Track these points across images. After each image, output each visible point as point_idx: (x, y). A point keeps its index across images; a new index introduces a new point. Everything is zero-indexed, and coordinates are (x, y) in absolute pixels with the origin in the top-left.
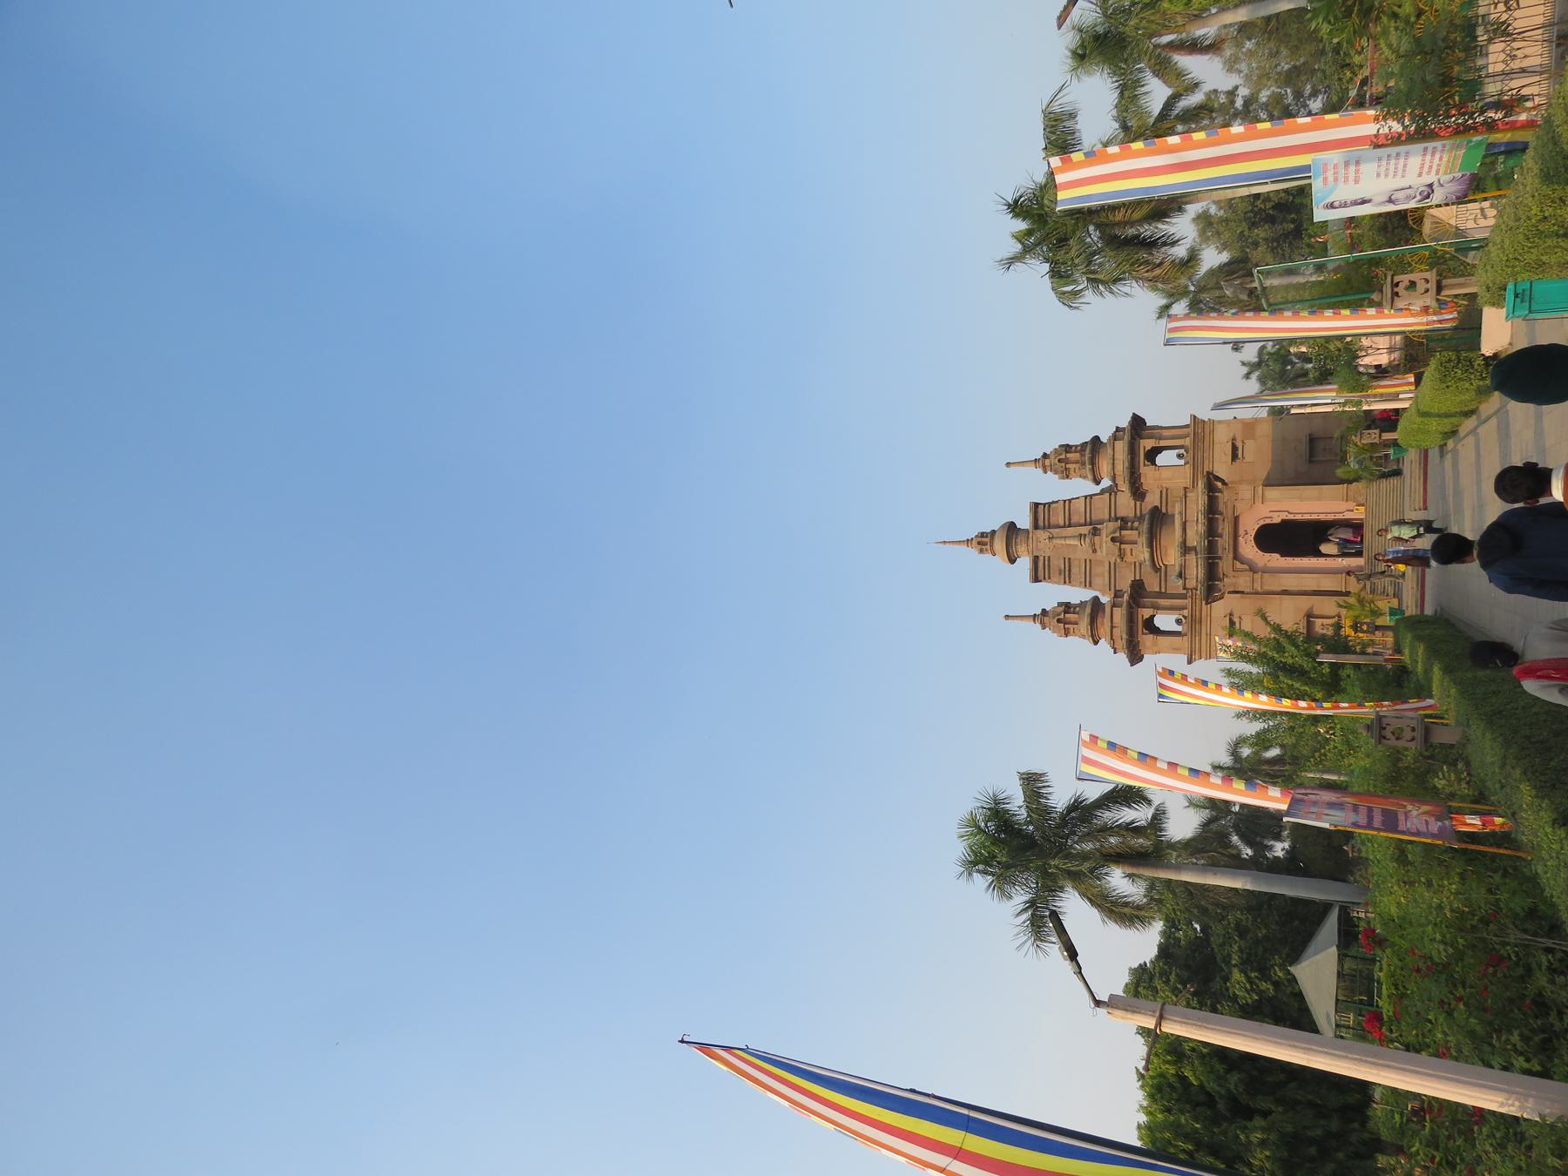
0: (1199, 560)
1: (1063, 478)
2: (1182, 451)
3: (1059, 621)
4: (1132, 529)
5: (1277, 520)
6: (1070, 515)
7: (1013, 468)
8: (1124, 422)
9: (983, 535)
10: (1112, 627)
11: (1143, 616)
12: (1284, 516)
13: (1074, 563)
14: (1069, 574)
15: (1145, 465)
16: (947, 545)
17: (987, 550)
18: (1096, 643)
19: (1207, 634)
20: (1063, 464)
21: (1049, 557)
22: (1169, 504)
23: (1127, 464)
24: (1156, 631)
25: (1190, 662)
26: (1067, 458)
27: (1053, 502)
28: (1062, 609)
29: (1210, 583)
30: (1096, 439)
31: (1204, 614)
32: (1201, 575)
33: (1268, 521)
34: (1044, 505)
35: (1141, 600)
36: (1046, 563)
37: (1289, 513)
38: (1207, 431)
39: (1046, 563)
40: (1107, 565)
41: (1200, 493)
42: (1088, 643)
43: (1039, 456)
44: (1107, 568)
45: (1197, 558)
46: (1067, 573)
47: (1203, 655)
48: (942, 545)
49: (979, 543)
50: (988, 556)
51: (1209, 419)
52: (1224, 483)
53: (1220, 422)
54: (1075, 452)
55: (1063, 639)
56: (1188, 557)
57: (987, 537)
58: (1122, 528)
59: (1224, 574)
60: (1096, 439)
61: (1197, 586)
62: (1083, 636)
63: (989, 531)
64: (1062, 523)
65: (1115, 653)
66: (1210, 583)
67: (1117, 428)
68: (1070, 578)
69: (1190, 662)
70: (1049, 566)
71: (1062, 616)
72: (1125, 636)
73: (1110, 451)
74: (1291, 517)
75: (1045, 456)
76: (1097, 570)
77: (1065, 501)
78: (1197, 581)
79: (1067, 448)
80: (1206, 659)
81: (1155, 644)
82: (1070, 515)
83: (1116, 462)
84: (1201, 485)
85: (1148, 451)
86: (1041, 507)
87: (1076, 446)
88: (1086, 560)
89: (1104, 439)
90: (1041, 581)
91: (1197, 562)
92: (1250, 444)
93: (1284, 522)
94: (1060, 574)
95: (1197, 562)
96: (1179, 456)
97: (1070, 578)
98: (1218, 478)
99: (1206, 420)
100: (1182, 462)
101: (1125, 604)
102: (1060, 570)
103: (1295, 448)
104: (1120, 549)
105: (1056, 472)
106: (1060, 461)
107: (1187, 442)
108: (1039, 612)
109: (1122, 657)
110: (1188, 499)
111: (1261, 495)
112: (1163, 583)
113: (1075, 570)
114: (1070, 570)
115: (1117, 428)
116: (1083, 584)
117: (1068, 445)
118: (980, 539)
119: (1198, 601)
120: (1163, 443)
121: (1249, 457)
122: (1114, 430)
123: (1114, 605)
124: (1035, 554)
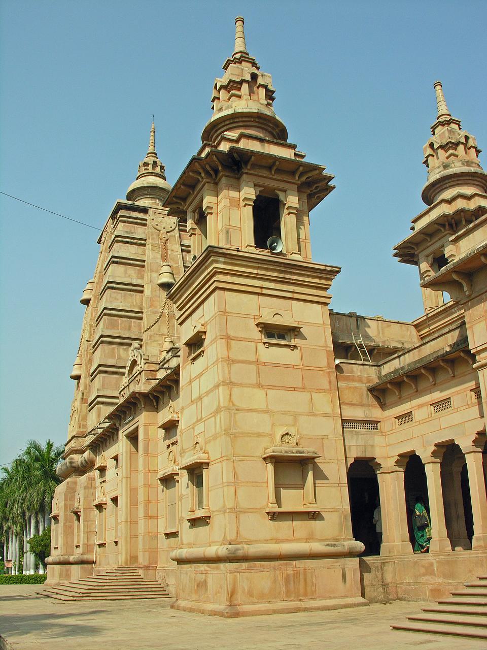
9: (162, 168)
11: (285, 191)
13: (139, 249)
17: (145, 169)
21: (145, 225)
36: (139, 221)
39: (139, 221)
40: (139, 282)
44: (134, 282)
49: (155, 163)
63: (166, 175)
76: (132, 271)
81: (234, 203)
88: (144, 261)
94: (127, 232)
97: (121, 242)
118: (159, 163)
119: (317, 281)
124: (150, 211)
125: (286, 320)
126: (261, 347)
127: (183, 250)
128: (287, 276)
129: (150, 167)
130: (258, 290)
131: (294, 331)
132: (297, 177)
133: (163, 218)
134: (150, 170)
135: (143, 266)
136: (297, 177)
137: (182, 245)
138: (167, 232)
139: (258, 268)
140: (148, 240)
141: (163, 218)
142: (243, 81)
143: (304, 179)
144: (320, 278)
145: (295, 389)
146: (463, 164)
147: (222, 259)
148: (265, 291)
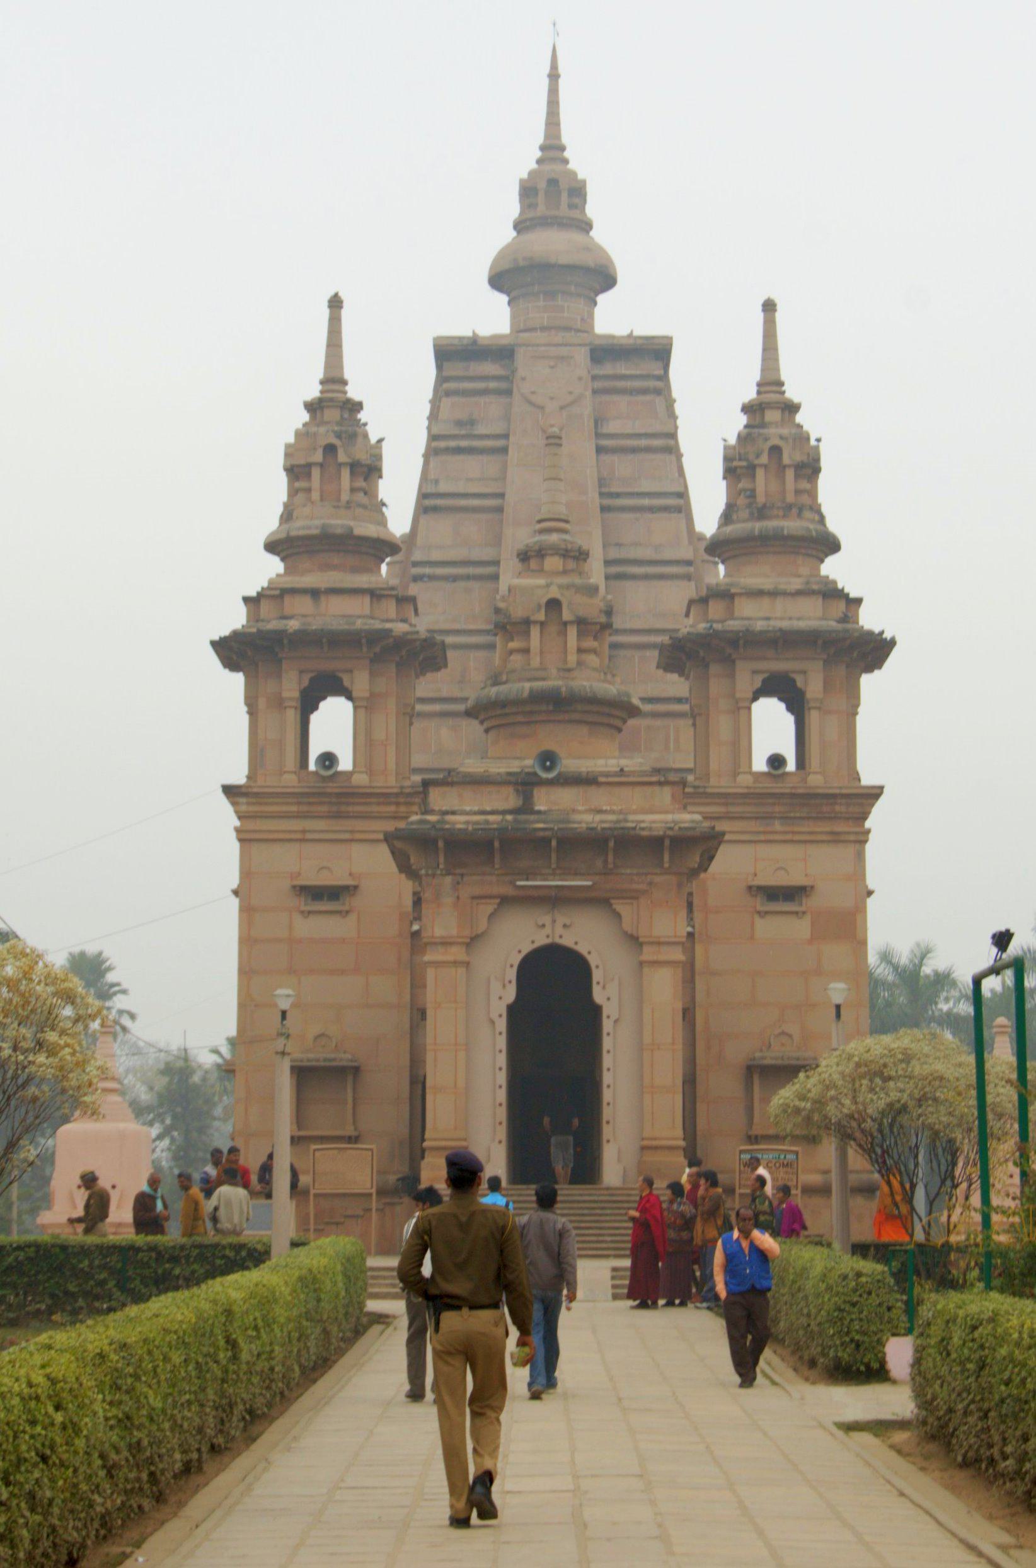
0: (498, 818)
1: (727, 459)
2: (791, 766)
3: (330, 449)
4: (580, 651)
5: (598, 996)
6: (634, 450)
7: (759, 317)
8: (869, 619)
9: (578, 192)
10: (315, 593)
11: (351, 671)
12: (609, 1011)
14: (459, 451)
15: (754, 672)
16: (545, 82)
18: (272, 547)
19: (304, 832)
20: (764, 459)
22: (658, 723)
23: (760, 626)
24: (309, 704)
25: (230, 791)
26: (783, 468)
27: (670, 403)
28: (362, 456)
29: (441, 844)
30: (832, 545)
31: (360, 825)
32: (459, 822)
33: (597, 975)
34: (664, 377)
35: (394, 670)
37: (616, 1021)
38: (840, 827)
40: (487, 554)
41: (669, 817)
42: (270, 523)
43: (792, 393)
45: (504, 812)
46: (464, 443)
47: (251, 825)
48: (546, 69)
50: (514, 209)
51: (868, 831)
52: (694, 873)
53: (860, 857)
54: (798, 492)
55: (278, 461)
56: (509, 791)
57: (571, 206)
58: (582, 623)
59: (462, 875)
60: (832, 545)
61: (432, 812)
62: (287, 516)
64: (612, 427)
65: (247, 600)
66: (441, 844)
67: (858, 601)
68: (448, 451)
69: (230, 791)
70: (485, 392)
71: (342, 457)
72: (293, 625)
73: (796, 584)
74: (607, 1025)
75: (792, 408)
77: (673, 436)
78: (446, 813)
79: (810, 468)
80: (238, 831)
82: (634, 450)
83: (766, 601)
84: (689, 818)
85: (794, 681)
86: (656, 369)
87: (813, 494)
89: (832, 568)
90: (439, 367)
91: (492, 813)
92: (801, 928)
93: (597, 1010)
94: (459, 423)
95: (492, 813)
96: (776, 761)
97: (448, 451)
98: (709, 858)
99: (868, 824)
100: (759, 764)
101: (378, 625)
102: (472, 422)
103: (783, 1033)
104: (527, 622)
105: (742, 439)
106: (776, 450)
107: (815, 781)
108: (353, 392)
109: (236, 619)
110: (657, 789)
111: (661, 958)
112: (437, 707)
113: (472, 466)
114: (470, 451)
115: (858, 601)
116: (430, 489)
117: (817, 470)
118: (564, 185)
119: (393, 808)
120: (813, 718)
121: (766, 928)
122: (853, 594)
123: (375, 595)
125: (337, 877)
126: (298, 920)
127: (600, 450)
128: (343, 808)
129: (541, 198)
130: (299, 836)
131: (349, 890)
132: (365, 649)
133: (552, 367)
134: (541, 210)
135: (500, 510)
136: (365, 649)
137: (598, 435)
138: (562, 408)
139: (299, 803)
140: (511, 438)
141: (552, 367)
142: (309, 466)
143: (377, 649)
144: (398, 804)
145: (343, 972)
146: (752, 514)
147: (243, 800)
148: (309, 836)
